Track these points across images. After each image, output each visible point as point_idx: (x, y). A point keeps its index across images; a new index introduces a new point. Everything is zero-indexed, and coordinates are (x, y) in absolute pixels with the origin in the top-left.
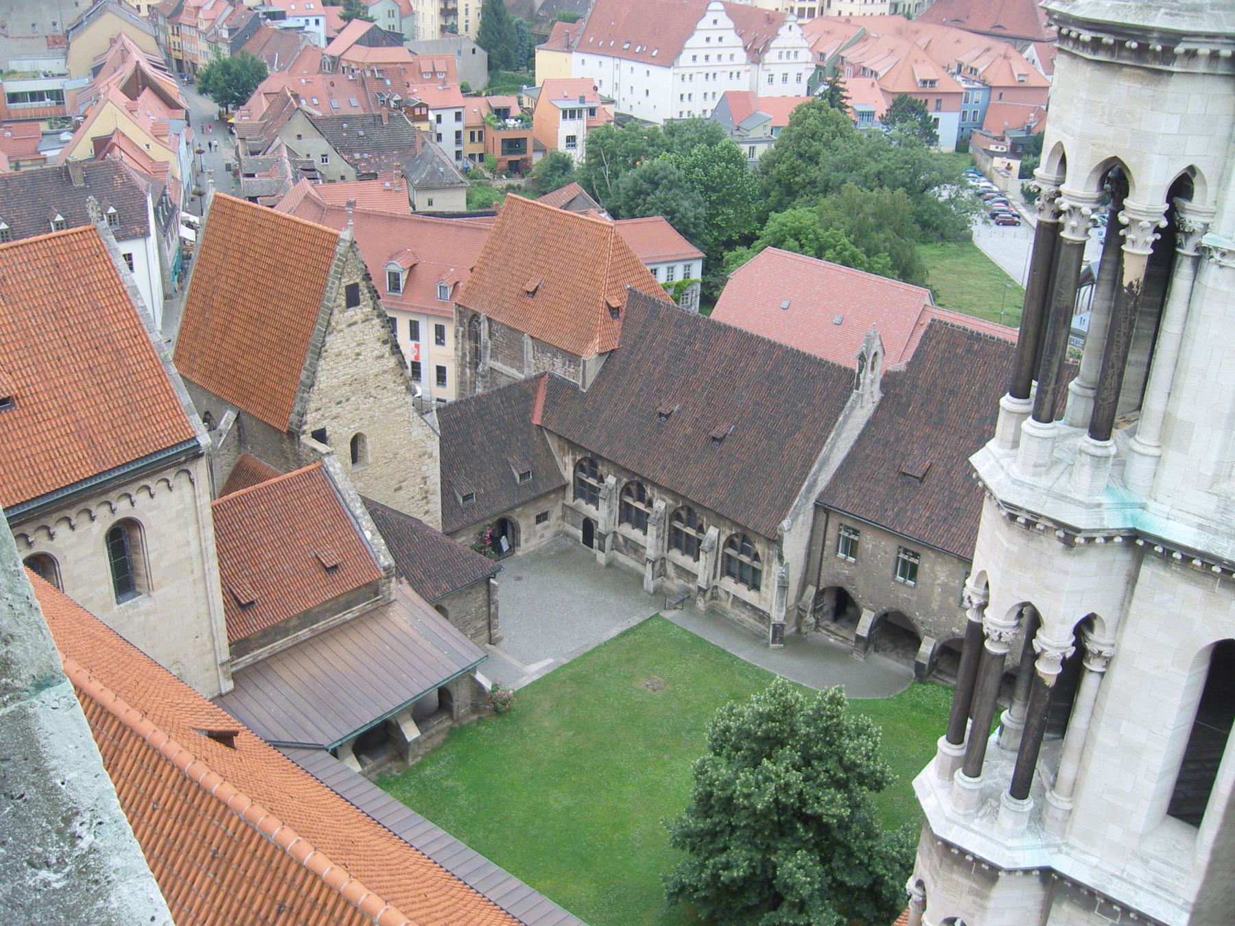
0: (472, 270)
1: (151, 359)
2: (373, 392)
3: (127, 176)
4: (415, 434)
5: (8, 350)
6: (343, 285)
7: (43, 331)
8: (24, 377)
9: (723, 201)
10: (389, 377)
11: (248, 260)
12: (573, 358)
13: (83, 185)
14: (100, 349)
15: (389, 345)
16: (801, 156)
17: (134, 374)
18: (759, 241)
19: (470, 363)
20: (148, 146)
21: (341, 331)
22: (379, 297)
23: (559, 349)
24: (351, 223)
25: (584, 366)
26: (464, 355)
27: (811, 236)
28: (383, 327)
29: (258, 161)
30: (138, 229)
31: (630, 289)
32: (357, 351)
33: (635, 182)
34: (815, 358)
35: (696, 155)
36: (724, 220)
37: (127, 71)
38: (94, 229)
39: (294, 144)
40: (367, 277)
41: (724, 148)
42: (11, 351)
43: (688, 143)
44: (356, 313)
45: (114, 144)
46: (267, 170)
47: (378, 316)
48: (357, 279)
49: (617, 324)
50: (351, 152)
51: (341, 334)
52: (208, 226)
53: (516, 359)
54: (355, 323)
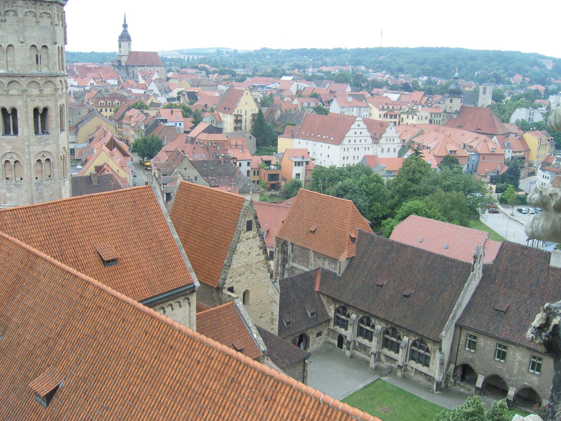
0: (283, 222)
4: (270, 291)
8: (121, 250)
9: (375, 200)
11: (197, 210)
12: (334, 260)
13: (97, 184)
15: (262, 249)
16: (409, 180)
17: (167, 252)
18: (398, 215)
19: (281, 264)
20: (118, 171)
23: (327, 256)
25: (340, 264)
26: (278, 260)
27: (423, 212)
28: (260, 241)
29: (168, 178)
31: (359, 230)
32: (249, 251)
33: (337, 190)
34: (451, 258)
35: (362, 179)
36: (375, 208)
37: (107, 139)
39: (183, 171)
40: (256, 218)
41: (374, 176)
43: (358, 175)
44: (250, 234)
45: (105, 169)
46: (172, 182)
47: (259, 236)
49: (354, 245)
52: (177, 195)
53: (306, 262)
54: (249, 238)
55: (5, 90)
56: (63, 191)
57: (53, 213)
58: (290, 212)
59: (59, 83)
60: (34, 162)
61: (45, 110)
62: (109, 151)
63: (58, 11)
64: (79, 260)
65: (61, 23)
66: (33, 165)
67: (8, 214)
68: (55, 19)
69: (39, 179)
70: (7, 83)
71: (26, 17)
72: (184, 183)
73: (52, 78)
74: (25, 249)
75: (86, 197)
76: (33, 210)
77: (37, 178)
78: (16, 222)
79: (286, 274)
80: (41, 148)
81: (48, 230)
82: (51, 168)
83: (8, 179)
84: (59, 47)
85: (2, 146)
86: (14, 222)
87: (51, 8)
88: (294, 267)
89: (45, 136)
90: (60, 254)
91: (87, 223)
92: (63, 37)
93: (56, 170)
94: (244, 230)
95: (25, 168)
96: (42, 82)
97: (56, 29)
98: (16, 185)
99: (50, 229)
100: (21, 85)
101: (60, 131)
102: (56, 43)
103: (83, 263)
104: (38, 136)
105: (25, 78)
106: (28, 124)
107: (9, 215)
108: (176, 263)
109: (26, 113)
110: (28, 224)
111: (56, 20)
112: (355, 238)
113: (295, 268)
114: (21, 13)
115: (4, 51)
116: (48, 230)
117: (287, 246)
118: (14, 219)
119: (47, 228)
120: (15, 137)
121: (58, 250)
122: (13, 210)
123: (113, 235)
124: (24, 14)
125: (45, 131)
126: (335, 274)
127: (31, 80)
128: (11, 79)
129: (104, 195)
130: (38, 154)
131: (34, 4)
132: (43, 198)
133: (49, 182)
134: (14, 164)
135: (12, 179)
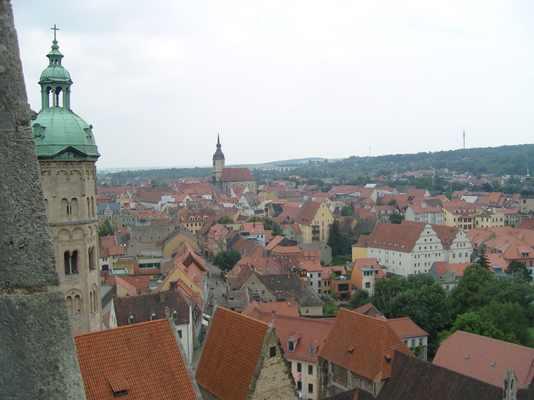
0: (325, 341)
2: (280, 395)
3: (182, 298)
5: (128, 369)
6: (269, 347)
7: (143, 362)
8: (133, 381)
9: (436, 310)
10: (288, 388)
12: (370, 382)
13: (164, 301)
14: (165, 371)
15: (288, 374)
16: (470, 289)
18: (453, 328)
19: (323, 383)
20: (191, 286)
21: (267, 367)
22: (284, 353)
23: (363, 377)
24: (273, 320)
25: (375, 386)
26: (321, 379)
27: (477, 325)
28: (285, 366)
30: (185, 320)
31: (395, 350)
32: (274, 376)
33: (396, 302)
34: (483, 382)
35: (423, 290)
36: (436, 318)
37: (186, 256)
38: (167, 320)
39: (251, 286)
40: (279, 344)
41: (435, 287)
42: (129, 370)
43: (419, 285)
44: (274, 360)
45: (178, 285)
46: (239, 297)
47: (284, 361)
48: (275, 345)
49: (390, 366)
50: (274, 289)
51: (267, 368)
52: (214, 320)
53: (344, 381)
54: (273, 364)
56: (92, 323)
58: (331, 331)
59: (89, 229)
61: (75, 253)
62: (184, 267)
64: (91, 391)
65: (91, 177)
68: (83, 176)
71: (58, 175)
72: (219, 308)
79: (328, 393)
80: (70, 287)
82: (80, 304)
84: (88, 198)
87: (80, 166)
88: (335, 386)
89: (75, 276)
91: (103, 356)
93: (85, 305)
94: (267, 356)
97: (84, 183)
100: (53, 233)
102: (84, 196)
103: (94, 394)
104: (68, 276)
108: (186, 393)
112: (390, 359)
113: (336, 387)
114: (53, 173)
117: (328, 365)
123: (126, 367)
124: (56, 173)
125: (75, 270)
126: (371, 395)
127: (62, 228)
129: (122, 329)
130: (68, 291)
131: (65, 164)
133: (78, 316)
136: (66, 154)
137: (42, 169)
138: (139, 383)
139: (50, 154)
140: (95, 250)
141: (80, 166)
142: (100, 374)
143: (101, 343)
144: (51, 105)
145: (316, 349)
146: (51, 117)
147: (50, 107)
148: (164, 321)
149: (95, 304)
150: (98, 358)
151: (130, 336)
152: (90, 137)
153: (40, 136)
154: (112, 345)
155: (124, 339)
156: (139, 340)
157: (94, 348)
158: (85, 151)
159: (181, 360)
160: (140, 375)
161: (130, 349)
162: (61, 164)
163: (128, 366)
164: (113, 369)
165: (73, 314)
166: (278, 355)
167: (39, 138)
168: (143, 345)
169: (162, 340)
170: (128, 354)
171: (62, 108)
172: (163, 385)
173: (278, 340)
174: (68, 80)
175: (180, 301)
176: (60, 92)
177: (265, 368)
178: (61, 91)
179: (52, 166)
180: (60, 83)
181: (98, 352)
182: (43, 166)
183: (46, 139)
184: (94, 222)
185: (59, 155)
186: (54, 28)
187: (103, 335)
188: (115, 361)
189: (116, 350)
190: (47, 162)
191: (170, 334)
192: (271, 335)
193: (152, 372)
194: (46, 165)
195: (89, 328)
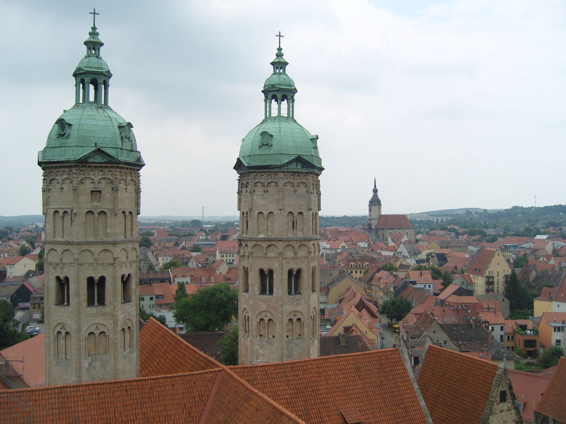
0: (542, 395)
1: (421, 414)
3: (364, 342)
5: (360, 401)
6: (499, 390)
14: (398, 406)
17: (413, 420)
20: (366, 332)
21: (497, 414)
29: (416, 341)
37: (357, 300)
38: (397, 350)
39: (432, 335)
40: (511, 388)
42: (361, 401)
44: (504, 406)
45: (353, 330)
47: (515, 408)
48: (506, 388)
50: (457, 340)
51: (496, 416)
52: (425, 360)
54: (503, 411)
55: (264, 253)
56: (311, 350)
57: (301, 371)
58: (550, 383)
59: (312, 246)
60: (286, 320)
61: (299, 271)
63: (312, 180)
65: (315, 191)
66: (285, 324)
67: (259, 370)
69: (290, 337)
70: (266, 246)
72: (432, 347)
73: (306, 241)
74: (272, 405)
75: (333, 358)
76: (282, 367)
77: (287, 337)
78: (266, 378)
80: (293, 308)
81: (294, 388)
82: (301, 328)
83: (261, 336)
84: (313, 213)
85: (258, 304)
86: (264, 378)
87: (307, 178)
89: (298, 297)
90: (305, 413)
92: (317, 204)
93: (306, 330)
95: (278, 327)
96: (296, 245)
97: (311, 197)
98: (269, 343)
99: (297, 387)
100: (278, 248)
101: (311, 291)
102: (311, 210)
104: (291, 296)
105: (282, 242)
106: (282, 284)
107: (260, 370)
109: (281, 274)
110: (276, 381)
111: (311, 189)
114: (281, 184)
115: (265, 217)
116: (294, 388)
118: (264, 375)
119: (294, 386)
120: (270, 296)
121: (303, 409)
122: (264, 366)
125: (297, 292)
128: (269, 243)
129: (351, 356)
130: (290, 313)
131: (293, 175)
132: (292, 356)
133: (298, 341)
134: (267, 322)
135: (265, 336)
136: (294, 164)
137: (268, 180)
138: (372, 416)
139: (279, 164)
140: (316, 271)
141: (307, 178)
142: (331, 403)
143: (331, 370)
144: (274, 113)
145: (523, 405)
146: (278, 126)
147: (272, 116)
148: (394, 351)
149: (313, 331)
150: (328, 386)
151: (360, 364)
152: (316, 148)
153: (268, 144)
154: (342, 373)
155: (354, 367)
156: (369, 370)
157: (323, 375)
158: (313, 161)
159: (415, 396)
160: (373, 408)
161: (360, 379)
162: (289, 175)
163: (359, 397)
164: (345, 399)
165: (294, 338)
166: (508, 401)
167: (267, 147)
168: (374, 375)
169: (393, 372)
170: (359, 384)
171: (287, 117)
172: (398, 421)
173: (509, 382)
174: (293, 88)
175: (362, 346)
176: (284, 101)
177: (494, 415)
178: (285, 100)
179: (279, 176)
180: (286, 91)
181: (328, 379)
182: (270, 177)
183: (274, 147)
184: (317, 239)
185: (287, 165)
186: (279, 35)
187: (332, 362)
188: (346, 390)
189: (347, 379)
190: (274, 172)
191: (401, 365)
192: (501, 376)
193: (385, 406)
194: (272, 175)
195: (309, 356)
